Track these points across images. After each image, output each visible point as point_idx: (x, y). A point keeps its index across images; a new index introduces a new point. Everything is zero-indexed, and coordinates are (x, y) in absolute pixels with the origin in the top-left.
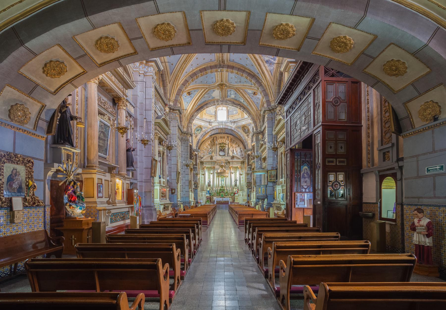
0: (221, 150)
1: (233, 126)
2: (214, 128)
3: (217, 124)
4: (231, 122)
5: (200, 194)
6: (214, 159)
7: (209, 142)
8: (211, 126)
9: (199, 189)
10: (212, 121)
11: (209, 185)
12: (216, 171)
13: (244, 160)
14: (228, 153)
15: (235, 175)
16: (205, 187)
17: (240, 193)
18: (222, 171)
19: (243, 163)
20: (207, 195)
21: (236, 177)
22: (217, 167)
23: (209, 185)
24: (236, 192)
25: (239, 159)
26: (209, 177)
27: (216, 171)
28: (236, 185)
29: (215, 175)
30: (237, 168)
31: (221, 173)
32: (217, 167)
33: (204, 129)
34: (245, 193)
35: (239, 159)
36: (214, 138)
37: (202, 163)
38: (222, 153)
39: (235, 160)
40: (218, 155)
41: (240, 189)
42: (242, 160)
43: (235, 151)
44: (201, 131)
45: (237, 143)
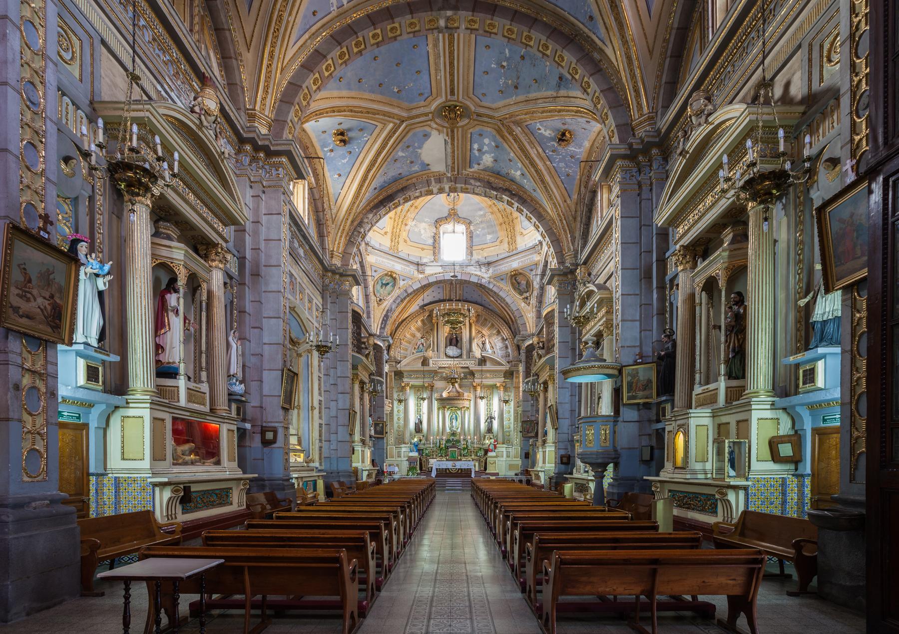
0: (451, 345)
1: (484, 275)
2: (432, 280)
3: (440, 270)
4: (480, 264)
5: (395, 451)
7: (419, 323)
8: (421, 276)
9: (391, 438)
10: (424, 261)
11: (418, 429)
12: (436, 395)
13: (513, 369)
14: (470, 350)
16: (407, 435)
17: (502, 449)
18: (454, 394)
19: (509, 374)
20: (412, 454)
22: (439, 384)
23: (418, 429)
24: (492, 447)
25: (500, 364)
26: (419, 411)
27: (436, 395)
28: (490, 430)
29: (435, 404)
30: (494, 387)
33: (402, 283)
34: (515, 449)
37: (399, 374)
39: (489, 366)
44: (394, 286)
45: (493, 325)
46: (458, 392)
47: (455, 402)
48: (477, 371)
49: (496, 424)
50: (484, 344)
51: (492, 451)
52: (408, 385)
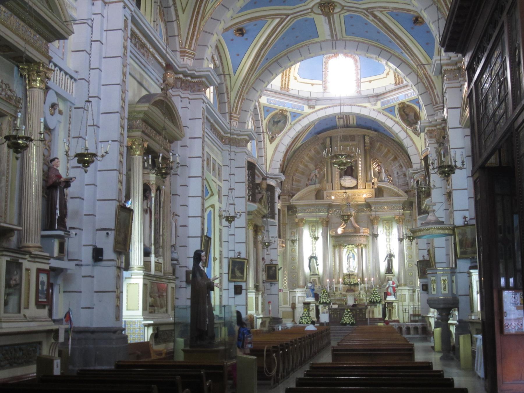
7: (313, 152)
15: (388, 241)
18: (351, 230)
22: (335, 219)
25: (399, 195)
28: (389, 270)
31: (344, 235)
32: (335, 219)
35: (399, 195)
36: (325, 139)
37: (292, 209)
38: (348, 181)
41: (403, 282)
42: (404, 198)
43: (383, 175)
46: (355, 228)
47: (351, 239)
48: (375, 203)
49: (396, 268)
50: (380, 173)
52: (302, 220)
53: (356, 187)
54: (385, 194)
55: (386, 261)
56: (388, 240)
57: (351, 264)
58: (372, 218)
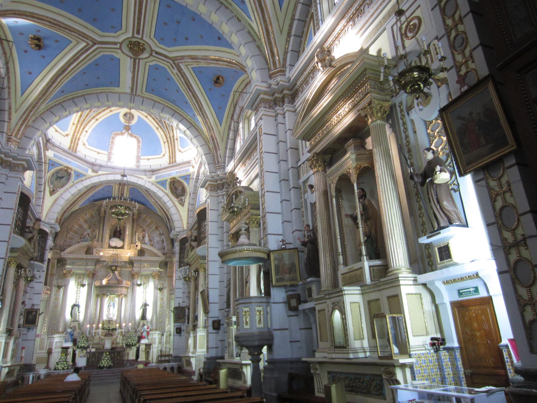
6: (95, 255)
13: (167, 260)
18: (114, 282)
21: (145, 299)
22: (101, 271)
25: (156, 255)
28: (144, 317)
31: (108, 286)
35: (156, 255)
37: (61, 262)
39: (146, 258)
40: (106, 246)
42: (162, 258)
43: (147, 239)
46: (118, 280)
47: (114, 289)
49: (149, 315)
51: (144, 338)
53: (122, 247)
54: (146, 254)
55: (142, 310)
56: (144, 292)
57: (111, 312)
58: (133, 273)
